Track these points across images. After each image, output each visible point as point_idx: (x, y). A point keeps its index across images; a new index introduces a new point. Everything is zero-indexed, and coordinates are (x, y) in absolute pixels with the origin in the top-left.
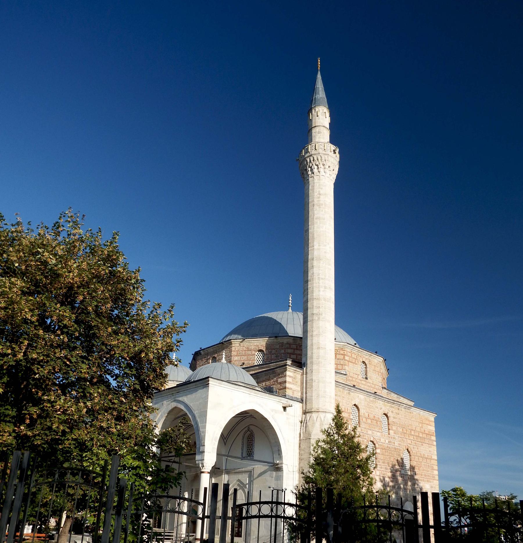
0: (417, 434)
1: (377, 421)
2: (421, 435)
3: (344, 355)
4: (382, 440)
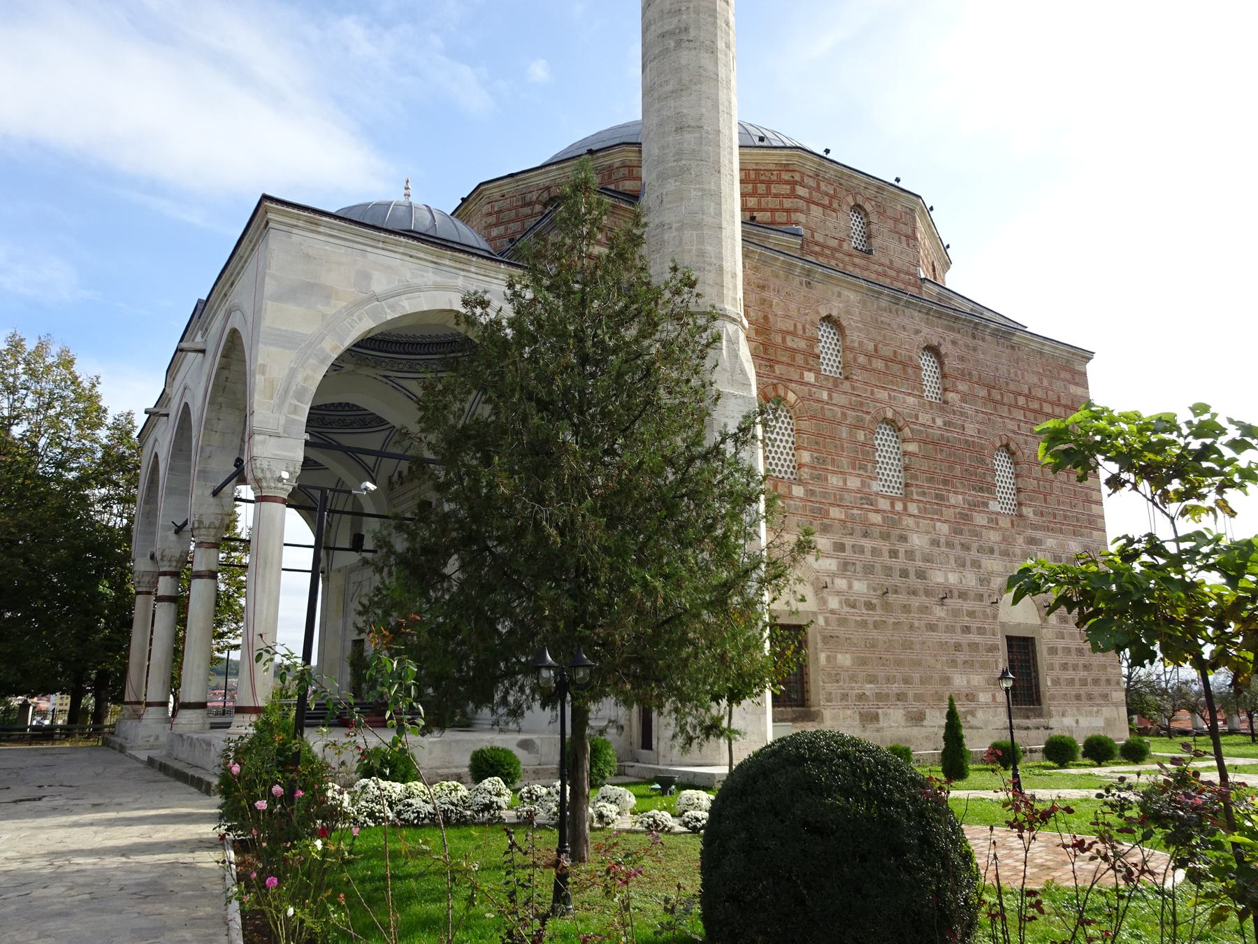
0: (1036, 406)
1: (904, 366)
3: (793, 183)
4: (924, 418)
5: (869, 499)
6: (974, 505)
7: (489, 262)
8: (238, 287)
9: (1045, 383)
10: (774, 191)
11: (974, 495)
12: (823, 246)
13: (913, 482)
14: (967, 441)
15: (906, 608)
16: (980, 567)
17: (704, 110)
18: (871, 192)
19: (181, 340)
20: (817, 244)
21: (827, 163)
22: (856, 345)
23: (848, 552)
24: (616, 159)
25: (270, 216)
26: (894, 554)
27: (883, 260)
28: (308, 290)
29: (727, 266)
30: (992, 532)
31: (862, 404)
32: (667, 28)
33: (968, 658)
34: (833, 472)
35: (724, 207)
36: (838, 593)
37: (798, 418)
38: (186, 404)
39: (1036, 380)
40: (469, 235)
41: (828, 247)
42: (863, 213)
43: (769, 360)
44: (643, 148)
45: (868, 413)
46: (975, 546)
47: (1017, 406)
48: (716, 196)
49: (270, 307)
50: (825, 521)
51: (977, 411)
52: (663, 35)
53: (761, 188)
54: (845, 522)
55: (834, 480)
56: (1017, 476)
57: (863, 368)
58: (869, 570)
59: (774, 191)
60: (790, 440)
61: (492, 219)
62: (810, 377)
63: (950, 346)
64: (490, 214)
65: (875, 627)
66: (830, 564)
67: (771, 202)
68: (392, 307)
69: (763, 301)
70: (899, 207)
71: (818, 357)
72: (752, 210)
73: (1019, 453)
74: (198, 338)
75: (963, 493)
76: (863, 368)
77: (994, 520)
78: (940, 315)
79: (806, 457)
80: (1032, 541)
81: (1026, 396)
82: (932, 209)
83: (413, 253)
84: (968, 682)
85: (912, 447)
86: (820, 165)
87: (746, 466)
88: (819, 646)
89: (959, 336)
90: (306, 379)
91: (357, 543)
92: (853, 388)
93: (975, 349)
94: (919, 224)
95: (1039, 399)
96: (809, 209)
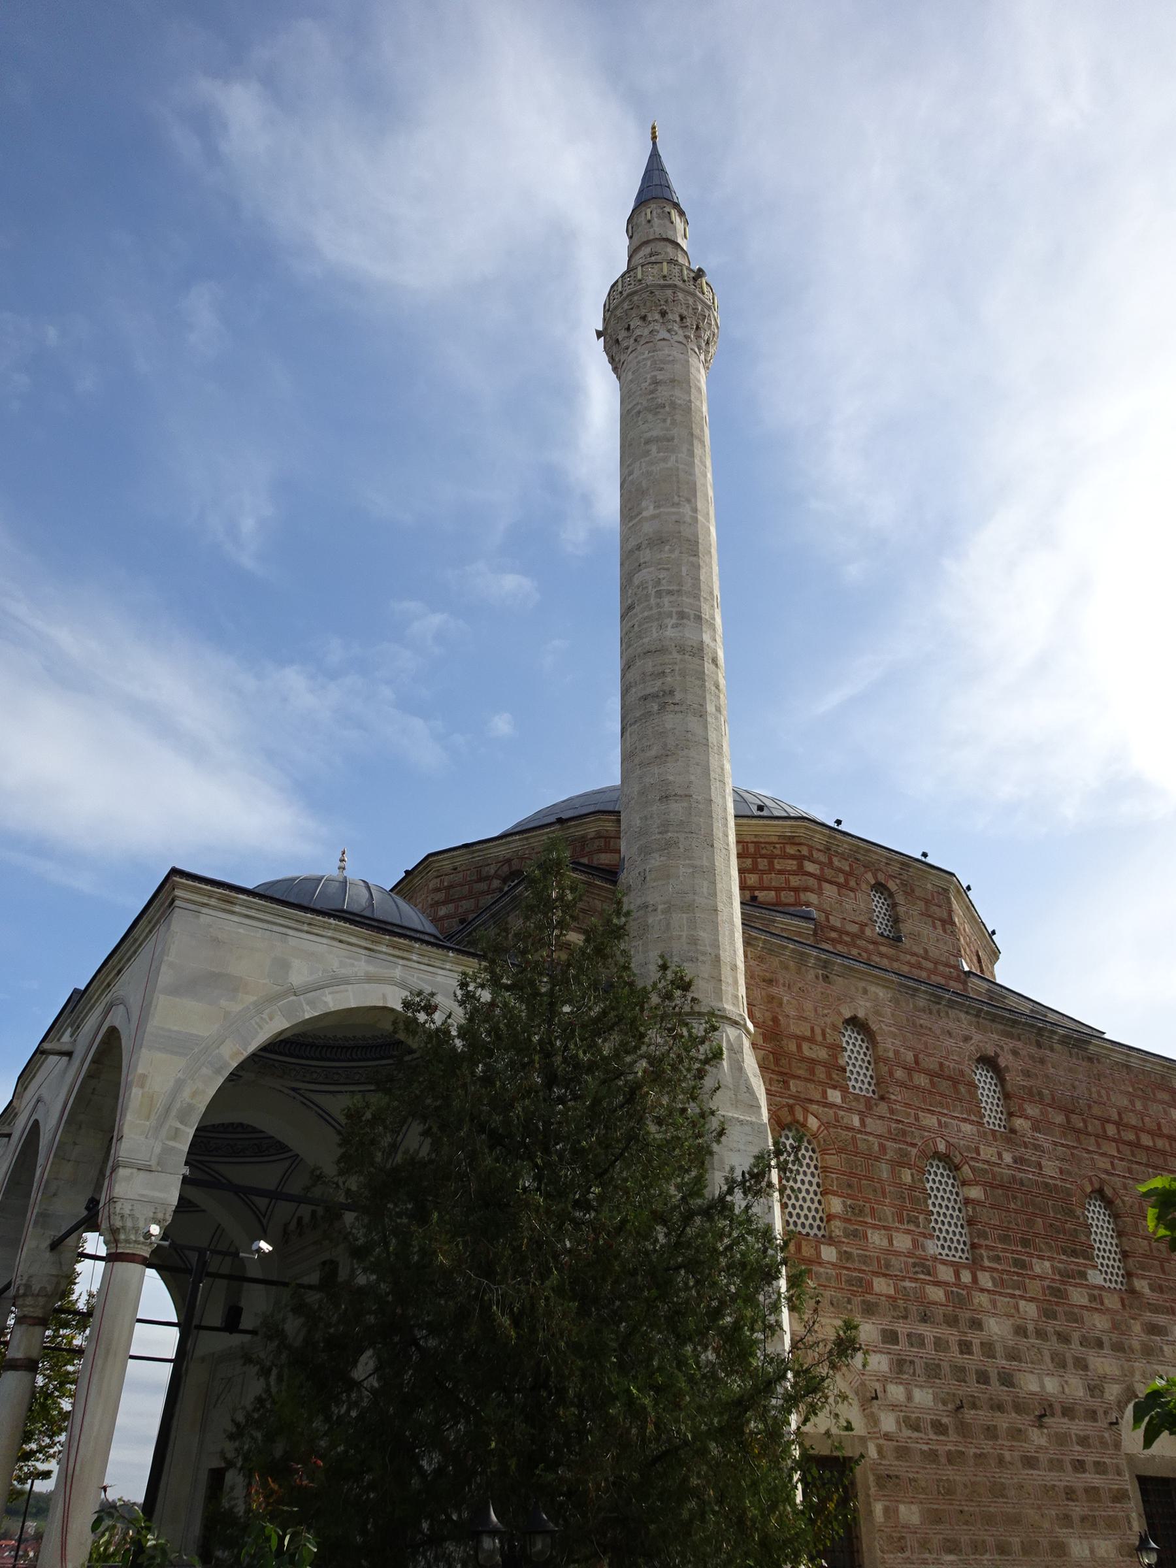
0: (1130, 1136)
1: (955, 1083)
2: (1146, 1140)
3: (800, 858)
5: (924, 1267)
6: (1067, 1276)
7: (434, 950)
8: (125, 976)
9: (1139, 1105)
10: (777, 867)
12: (841, 932)
13: (983, 1242)
14: (1047, 1185)
15: (991, 1432)
16: (1086, 1368)
17: (693, 778)
18: (896, 867)
19: (43, 1041)
20: (833, 929)
21: (839, 836)
22: (891, 1055)
23: (903, 1345)
24: (591, 829)
25: (178, 892)
26: (965, 1347)
27: (915, 949)
28: (210, 982)
29: (725, 956)
30: (1096, 1316)
31: (904, 1133)
32: (649, 691)
33: (1086, 1512)
34: (875, 1227)
35: (719, 886)
36: (894, 1407)
37: (824, 1152)
38: (36, 1121)
40: (411, 915)
41: (848, 933)
42: (886, 893)
43: (781, 1074)
44: (623, 815)
45: (914, 1145)
46: (1076, 1336)
47: (1106, 1137)
48: (710, 873)
49: (162, 1002)
50: (868, 1297)
51: (1055, 1144)
52: (645, 698)
53: (763, 864)
54: (895, 1299)
55: (876, 1239)
56: (1120, 1234)
57: (902, 1085)
58: (933, 1371)
59: (777, 867)
60: (815, 1181)
61: (440, 896)
62: (835, 1096)
63: (1011, 1057)
64: (437, 890)
65: (949, 1461)
66: (879, 1363)
67: (776, 880)
68: (311, 1003)
69: (771, 999)
70: (929, 886)
71: (844, 1070)
72: (752, 889)
73: (1118, 1201)
74: (66, 1038)
75: (1051, 1259)
76: (902, 1085)
77: (1096, 1295)
78: (994, 1018)
79: (836, 1205)
80: (1153, 1329)
81: (1117, 1124)
82: (969, 888)
83: (344, 937)
84: (1092, 1551)
85: (975, 1193)
86: (830, 837)
87: (761, 1225)
88: (873, 1491)
89: (1019, 1044)
90: (194, 1094)
91: (232, 1322)
92: (892, 1111)
93: (1042, 1061)
94: (955, 905)
95: (1134, 1127)
96: (820, 888)
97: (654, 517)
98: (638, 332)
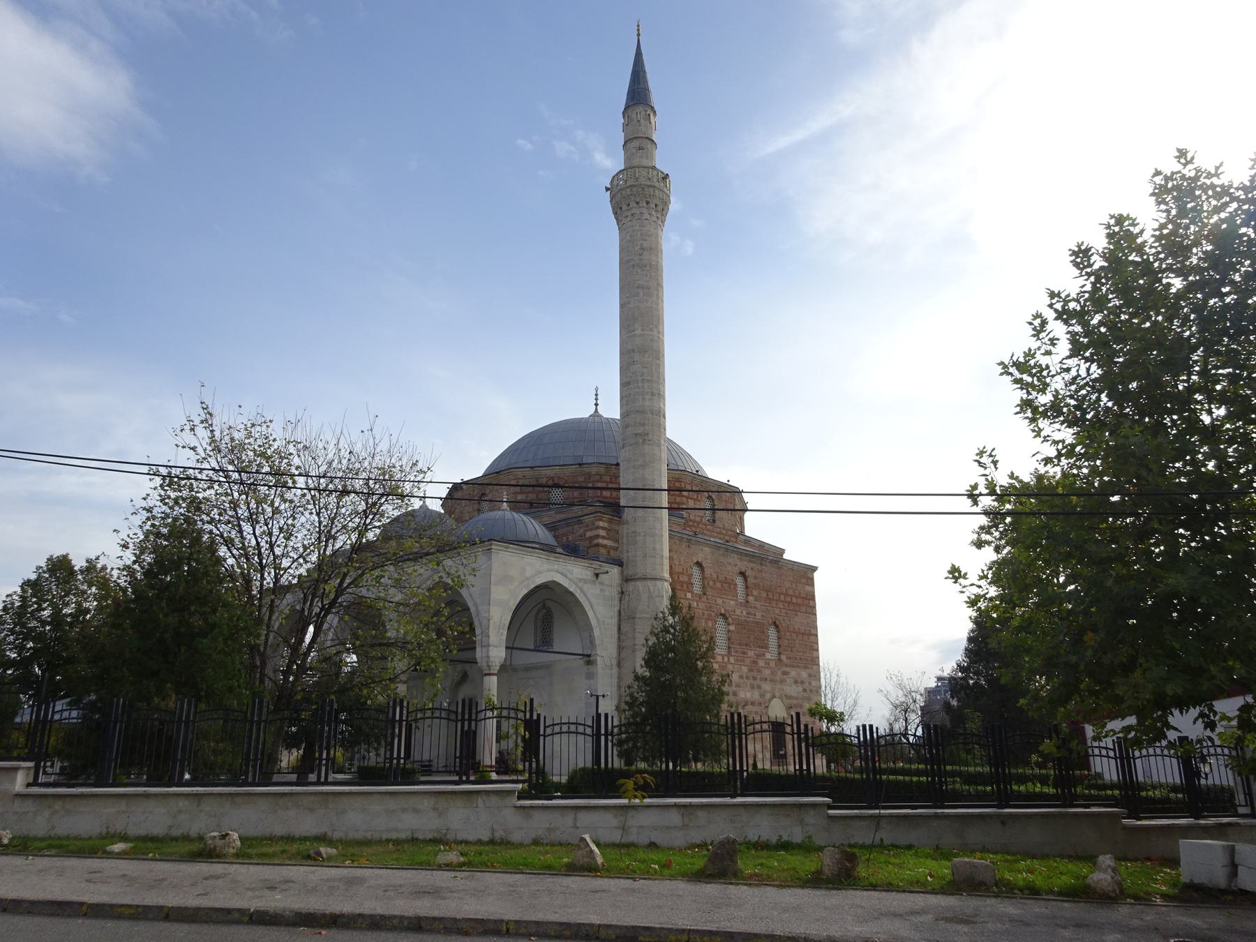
2: (794, 600)
6: (758, 656)
11: (759, 651)
39: (788, 585)
49: (493, 588)
78: (747, 555)
80: (785, 673)
85: (732, 628)
97: (642, 335)
98: (634, 211)
